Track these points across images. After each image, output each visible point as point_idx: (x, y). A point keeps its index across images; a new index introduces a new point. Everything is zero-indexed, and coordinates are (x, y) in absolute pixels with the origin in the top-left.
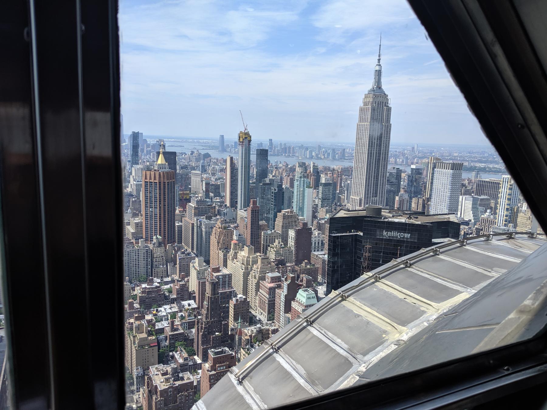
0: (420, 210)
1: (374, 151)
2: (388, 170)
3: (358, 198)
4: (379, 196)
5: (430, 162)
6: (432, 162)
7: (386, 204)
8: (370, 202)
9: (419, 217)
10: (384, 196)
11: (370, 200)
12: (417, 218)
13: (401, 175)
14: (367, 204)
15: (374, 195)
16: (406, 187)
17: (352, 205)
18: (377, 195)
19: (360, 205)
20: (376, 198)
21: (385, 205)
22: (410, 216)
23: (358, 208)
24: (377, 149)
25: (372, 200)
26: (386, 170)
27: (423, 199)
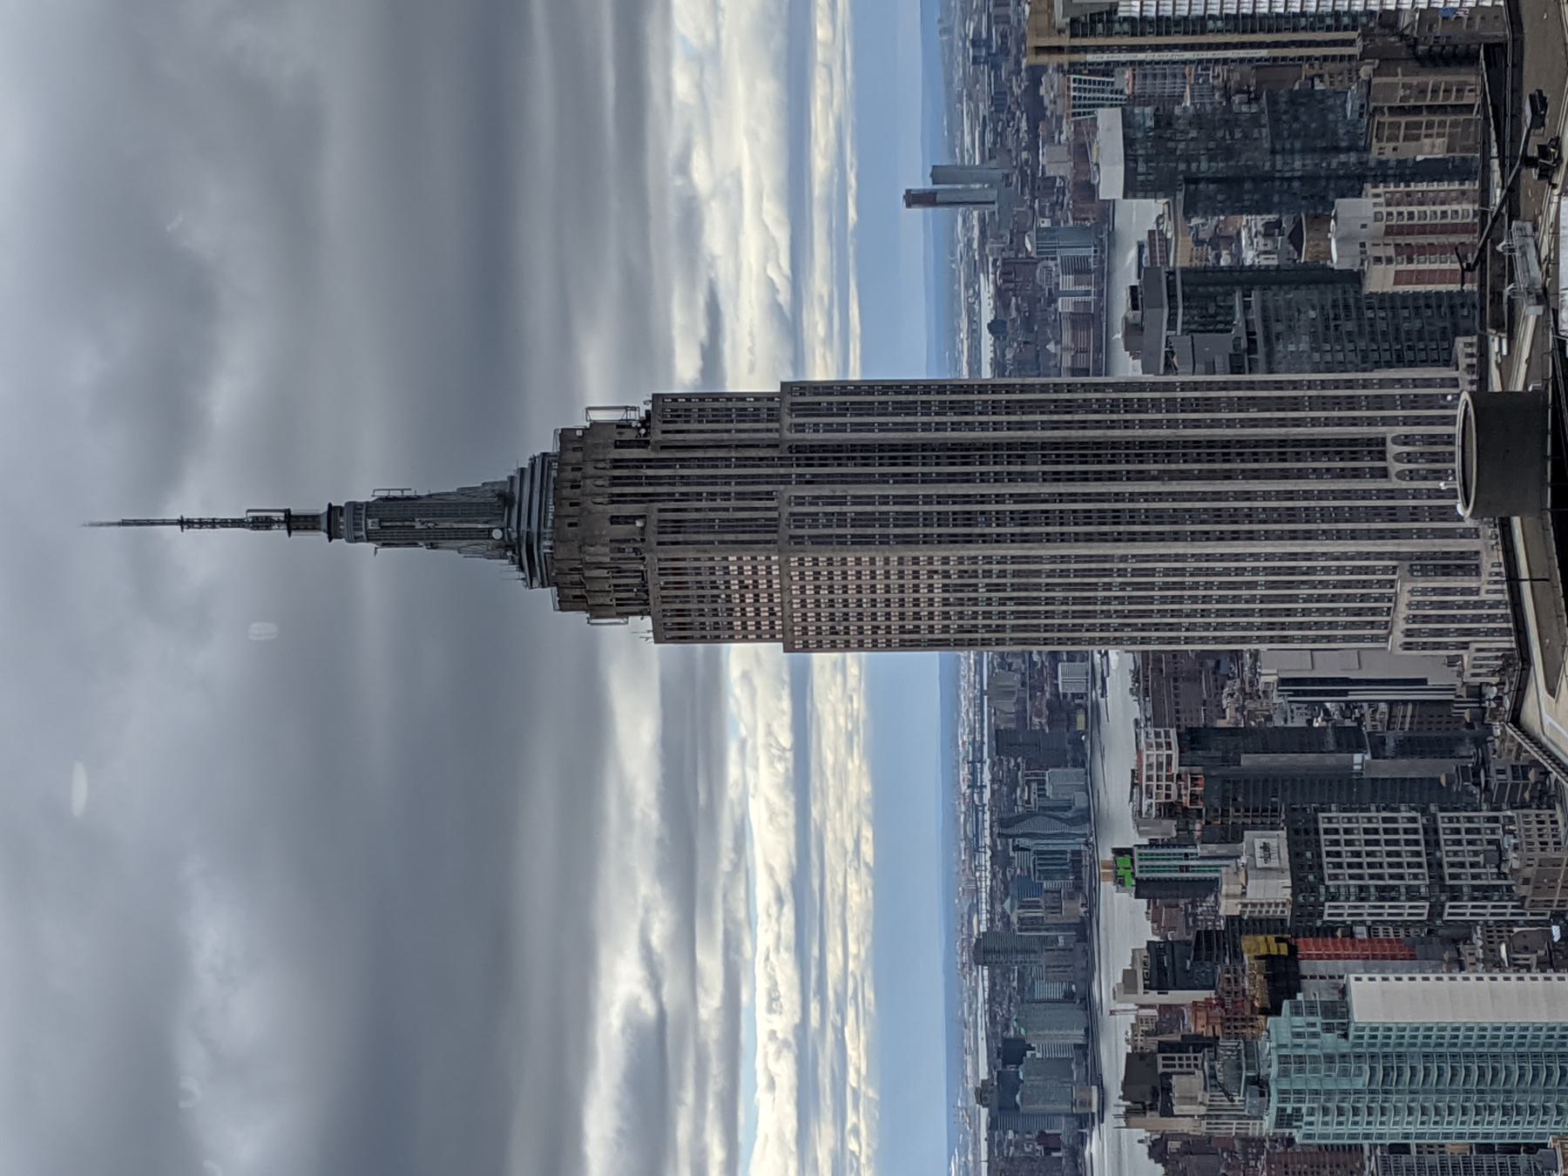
0: (1471, 84)
1: (999, 499)
2: (1151, 378)
3: (1406, 590)
4: (1371, 422)
5: (1065, 59)
6: (1065, 41)
7: (1435, 363)
8: (1439, 494)
9: (1528, 89)
10: (1366, 384)
11: (1416, 494)
12: (1539, 103)
13: (1184, 271)
14: (1447, 513)
15: (1366, 464)
16: (1278, 224)
17: (1468, 632)
18: (1369, 442)
19: (1466, 565)
20: (1393, 449)
21: (1453, 374)
22: (1529, 162)
23: (1488, 587)
24: (984, 478)
25: (1412, 476)
26: (1154, 387)
27: (1377, 72)
